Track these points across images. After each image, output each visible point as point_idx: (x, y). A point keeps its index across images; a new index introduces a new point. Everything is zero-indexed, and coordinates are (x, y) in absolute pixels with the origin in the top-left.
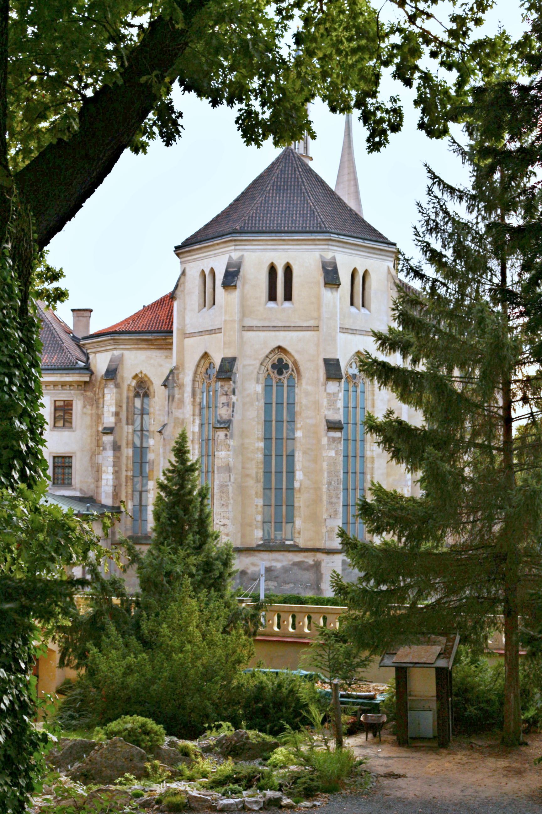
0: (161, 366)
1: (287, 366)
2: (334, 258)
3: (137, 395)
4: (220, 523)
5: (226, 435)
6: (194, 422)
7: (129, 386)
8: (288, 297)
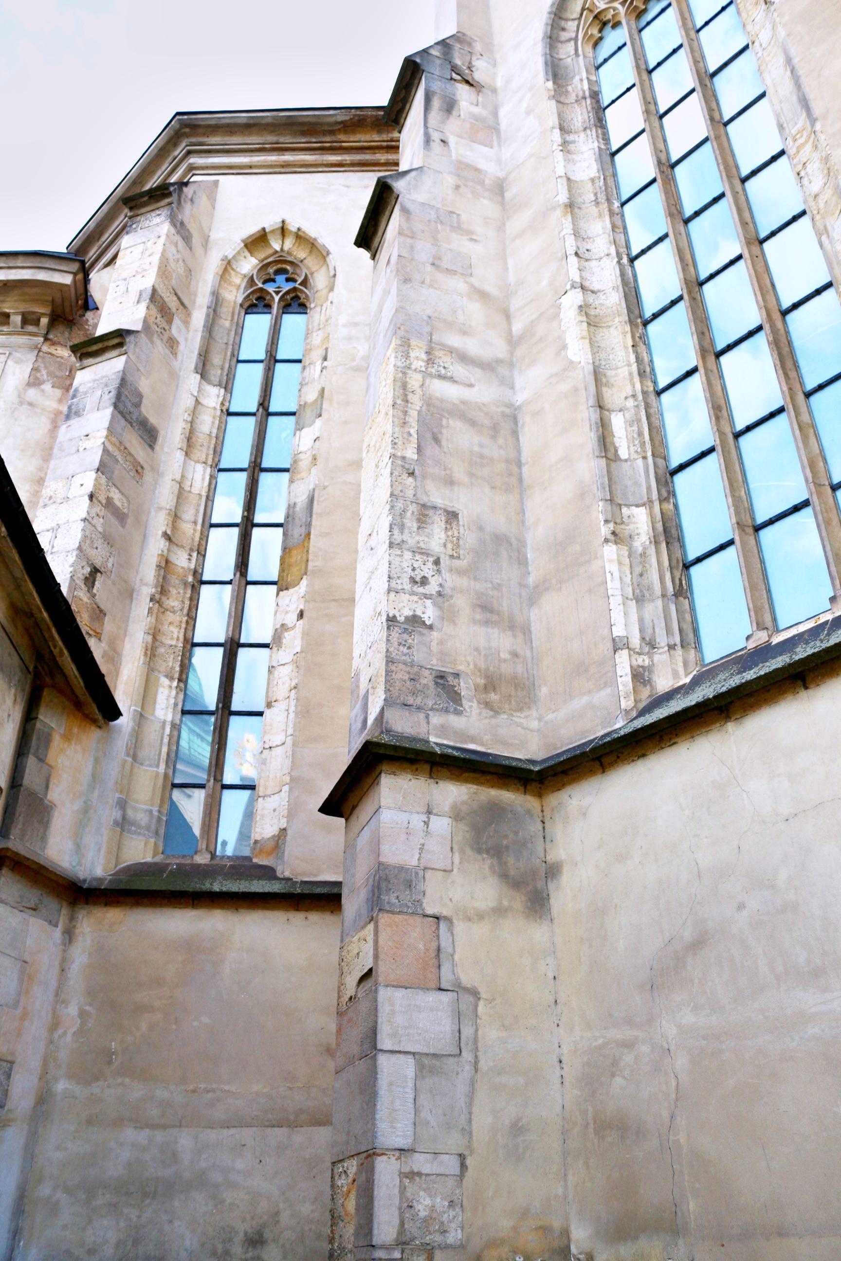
3: (257, 302)
7: (228, 265)
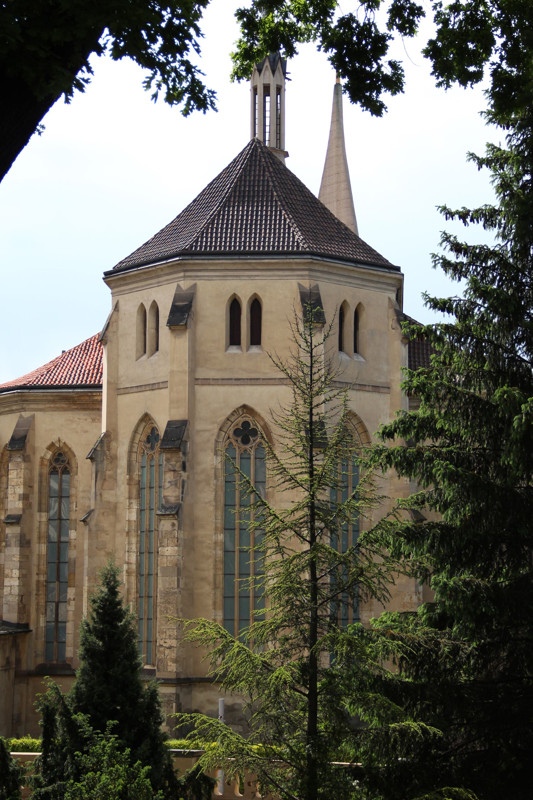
0: (86, 432)
1: (254, 432)
2: (317, 287)
3: (53, 471)
4: (164, 645)
5: (173, 525)
6: (130, 507)
8: (256, 339)
